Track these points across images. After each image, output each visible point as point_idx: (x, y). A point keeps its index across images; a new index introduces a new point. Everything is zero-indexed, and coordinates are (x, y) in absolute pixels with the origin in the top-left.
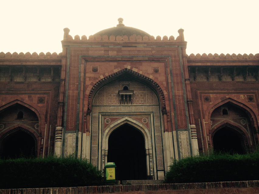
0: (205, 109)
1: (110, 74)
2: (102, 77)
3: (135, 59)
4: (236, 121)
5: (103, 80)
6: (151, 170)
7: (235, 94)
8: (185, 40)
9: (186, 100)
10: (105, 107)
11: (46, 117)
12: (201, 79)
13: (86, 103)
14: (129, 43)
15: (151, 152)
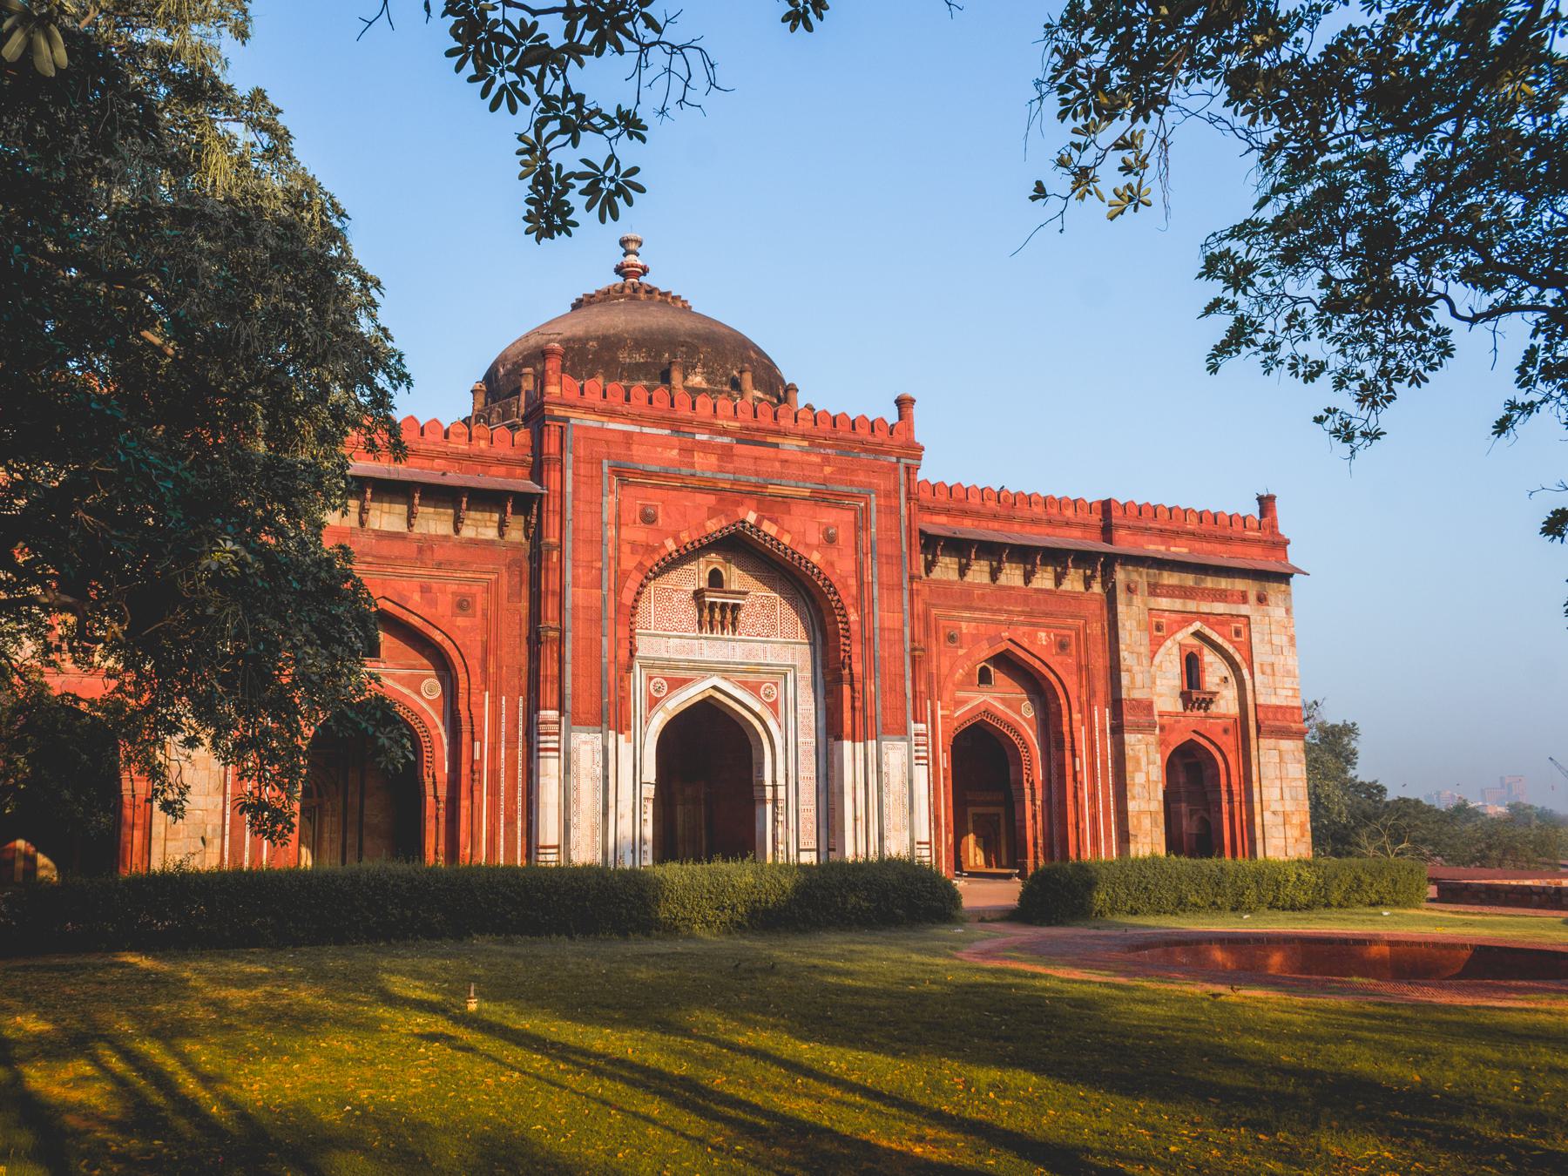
0: (945, 670)
1: (696, 537)
2: (671, 545)
3: (771, 489)
4: (1009, 707)
5: (675, 555)
6: (781, 847)
7: (1026, 629)
8: (919, 437)
9: (908, 646)
10: (654, 640)
11: (485, 669)
12: (947, 568)
13: (623, 632)
14: (758, 430)
15: (781, 794)
